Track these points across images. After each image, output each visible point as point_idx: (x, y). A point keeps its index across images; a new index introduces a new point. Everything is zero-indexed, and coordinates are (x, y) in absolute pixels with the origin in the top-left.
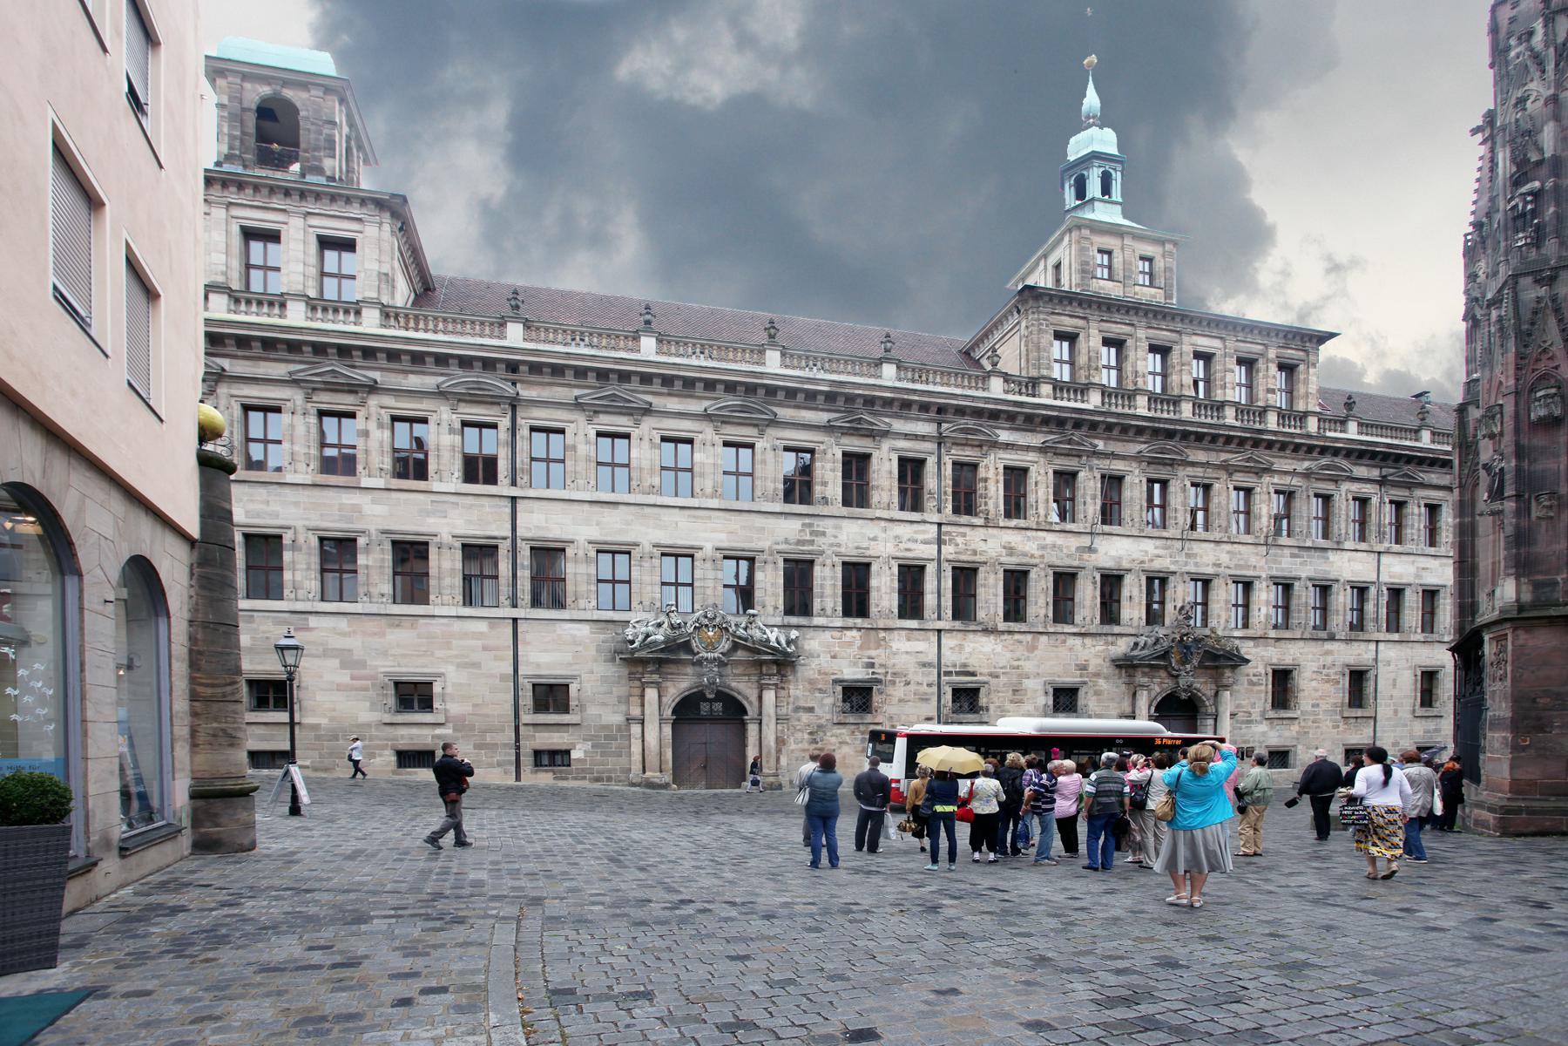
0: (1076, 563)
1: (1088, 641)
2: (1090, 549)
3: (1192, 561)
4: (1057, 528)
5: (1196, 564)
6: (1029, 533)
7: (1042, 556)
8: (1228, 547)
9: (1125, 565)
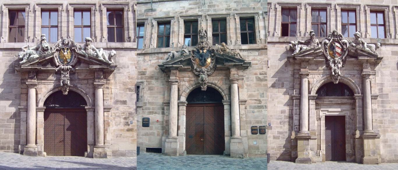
0: (144, 17)
1: (147, 58)
2: (152, 10)
3: (212, 9)
5: (215, 10)
9: (171, 15)
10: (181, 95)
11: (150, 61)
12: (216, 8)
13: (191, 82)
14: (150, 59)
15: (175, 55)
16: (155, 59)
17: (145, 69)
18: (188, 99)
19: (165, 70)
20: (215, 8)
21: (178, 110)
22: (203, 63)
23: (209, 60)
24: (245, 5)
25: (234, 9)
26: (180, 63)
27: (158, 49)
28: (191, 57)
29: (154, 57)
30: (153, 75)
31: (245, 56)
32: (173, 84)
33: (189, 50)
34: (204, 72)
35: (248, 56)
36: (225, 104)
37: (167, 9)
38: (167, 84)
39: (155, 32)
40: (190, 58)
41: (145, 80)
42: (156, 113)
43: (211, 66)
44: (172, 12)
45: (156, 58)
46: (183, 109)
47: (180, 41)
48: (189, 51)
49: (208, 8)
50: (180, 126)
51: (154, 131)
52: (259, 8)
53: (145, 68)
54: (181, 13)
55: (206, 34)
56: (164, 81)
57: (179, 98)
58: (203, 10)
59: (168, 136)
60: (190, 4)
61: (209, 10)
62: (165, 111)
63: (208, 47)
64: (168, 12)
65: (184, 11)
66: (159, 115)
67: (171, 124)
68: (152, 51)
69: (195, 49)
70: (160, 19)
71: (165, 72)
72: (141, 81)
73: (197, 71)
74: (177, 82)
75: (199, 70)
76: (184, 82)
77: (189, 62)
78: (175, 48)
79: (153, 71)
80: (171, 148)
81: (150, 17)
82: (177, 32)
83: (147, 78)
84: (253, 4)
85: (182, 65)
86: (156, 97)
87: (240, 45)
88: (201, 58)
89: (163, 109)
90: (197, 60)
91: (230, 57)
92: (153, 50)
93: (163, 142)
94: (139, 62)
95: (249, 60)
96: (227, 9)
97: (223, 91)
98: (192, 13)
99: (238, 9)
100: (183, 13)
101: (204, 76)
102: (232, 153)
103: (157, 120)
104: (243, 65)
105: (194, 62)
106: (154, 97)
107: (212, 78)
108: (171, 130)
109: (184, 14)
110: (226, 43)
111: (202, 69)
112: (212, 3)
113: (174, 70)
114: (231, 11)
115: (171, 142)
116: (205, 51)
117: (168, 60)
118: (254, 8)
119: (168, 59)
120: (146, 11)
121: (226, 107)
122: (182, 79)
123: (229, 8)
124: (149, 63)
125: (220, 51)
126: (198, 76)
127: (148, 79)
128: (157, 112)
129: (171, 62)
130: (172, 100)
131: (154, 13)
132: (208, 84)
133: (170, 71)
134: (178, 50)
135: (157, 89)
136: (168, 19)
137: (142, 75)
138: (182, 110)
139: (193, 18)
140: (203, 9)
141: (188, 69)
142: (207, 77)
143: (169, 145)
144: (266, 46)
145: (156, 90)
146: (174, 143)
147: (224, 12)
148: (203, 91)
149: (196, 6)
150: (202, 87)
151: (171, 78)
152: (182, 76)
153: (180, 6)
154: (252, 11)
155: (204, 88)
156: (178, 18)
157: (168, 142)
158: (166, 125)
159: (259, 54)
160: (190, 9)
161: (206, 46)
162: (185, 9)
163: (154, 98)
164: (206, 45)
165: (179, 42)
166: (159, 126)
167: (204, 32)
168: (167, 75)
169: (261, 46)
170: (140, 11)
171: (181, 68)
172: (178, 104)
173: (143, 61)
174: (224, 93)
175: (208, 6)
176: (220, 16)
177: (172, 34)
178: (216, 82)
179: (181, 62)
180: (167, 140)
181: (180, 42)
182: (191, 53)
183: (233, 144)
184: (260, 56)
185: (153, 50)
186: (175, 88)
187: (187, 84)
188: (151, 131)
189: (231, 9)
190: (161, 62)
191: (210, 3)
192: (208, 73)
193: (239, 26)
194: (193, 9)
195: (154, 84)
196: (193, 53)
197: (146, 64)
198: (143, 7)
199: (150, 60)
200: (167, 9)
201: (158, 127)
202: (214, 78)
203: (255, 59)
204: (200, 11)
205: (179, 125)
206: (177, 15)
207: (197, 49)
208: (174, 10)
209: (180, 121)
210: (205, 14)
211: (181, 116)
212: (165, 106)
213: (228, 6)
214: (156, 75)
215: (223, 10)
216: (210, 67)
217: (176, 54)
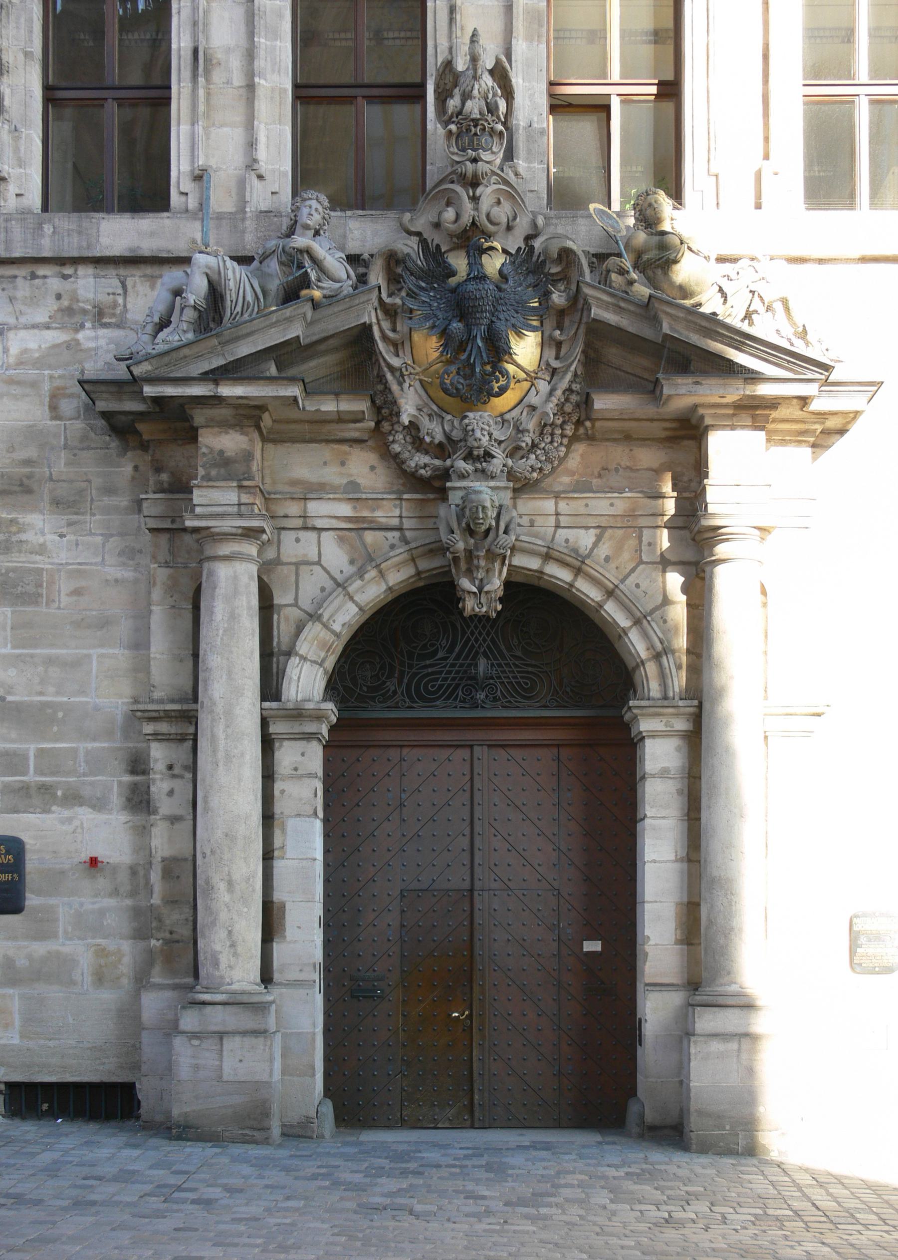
10: (289, 654)
13: (370, 537)
15: (230, 298)
16: (41, 317)
18: (339, 684)
19: (144, 425)
21: (268, 776)
22: (475, 367)
26: (273, 370)
27: (65, 222)
28: (370, 315)
29: (33, 301)
30: (28, 462)
32: (226, 549)
33: (354, 247)
34: (488, 456)
36: (654, 735)
38: (163, 555)
39: (28, 55)
40: (365, 330)
42: (73, 798)
43: (546, 397)
45: (52, 305)
46: (304, 764)
47: (262, 154)
48: (353, 259)
50: (283, 906)
51: (66, 950)
55: (502, 105)
56: (134, 519)
57: (270, 687)
59: (191, 988)
62: (160, 786)
63: (522, 226)
66: (102, 817)
67: (210, 887)
69: (409, 246)
71: (144, 446)
73: (418, 444)
74: (251, 534)
75: (439, 437)
76: (313, 535)
77: (358, 360)
79: (32, 434)
80: (220, 1078)
82: (236, 63)
85: (294, 391)
86: (76, 664)
88: (456, 326)
89: (138, 765)
90: (429, 347)
92: (14, 225)
93: (146, 1037)
97: (637, 622)
101: (488, 494)
102: (700, 1113)
103: (85, 856)
104: (816, 406)
105: (395, 362)
106: (50, 661)
107: (549, 505)
108: (214, 942)
111: (467, 432)
113: (225, 425)
115: (221, 1035)
116: (493, 264)
117: (170, 337)
119: (164, 324)
121: (660, 755)
122: (293, 509)
125: (622, 272)
126: (432, 487)
128: (86, 792)
129: (199, 357)
130: (216, 690)
132: (520, 561)
133: (191, 436)
134: (250, 243)
135: (77, 592)
138: (297, 775)
141: (341, 418)
142: (506, 497)
143: (208, 1058)
145: (65, 600)
146: (249, 1041)
148: (474, 617)
151: (198, 496)
152: (294, 483)
155: (482, 593)
157: (194, 1035)
158: (171, 901)
161: (502, 213)
163: (55, 672)
165: (251, 164)
166: (107, 906)
167: (487, 81)
168: (158, 470)
171: (293, 414)
172: (264, 723)
174: (645, 635)
177: (186, 85)
178: (585, 539)
179: (286, 355)
180: (189, 1020)
181: (264, 166)
182: (377, 277)
183: (716, 1046)
185: (16, 229)
186: (233, 586)
187: (336, 557)
188: (40, 949)
190: (100, 349)
192: (522, 466)
195: (42, 550)
196: (394, 279)
201: (102, 912)
202: (563, 506)
205: (278, 896)
207: (423, 242)
209: (278, 865)
211: (291, 823)
212: (157, 737)
214: (60, 465)
216: (533, 408)
217: (236, 277)
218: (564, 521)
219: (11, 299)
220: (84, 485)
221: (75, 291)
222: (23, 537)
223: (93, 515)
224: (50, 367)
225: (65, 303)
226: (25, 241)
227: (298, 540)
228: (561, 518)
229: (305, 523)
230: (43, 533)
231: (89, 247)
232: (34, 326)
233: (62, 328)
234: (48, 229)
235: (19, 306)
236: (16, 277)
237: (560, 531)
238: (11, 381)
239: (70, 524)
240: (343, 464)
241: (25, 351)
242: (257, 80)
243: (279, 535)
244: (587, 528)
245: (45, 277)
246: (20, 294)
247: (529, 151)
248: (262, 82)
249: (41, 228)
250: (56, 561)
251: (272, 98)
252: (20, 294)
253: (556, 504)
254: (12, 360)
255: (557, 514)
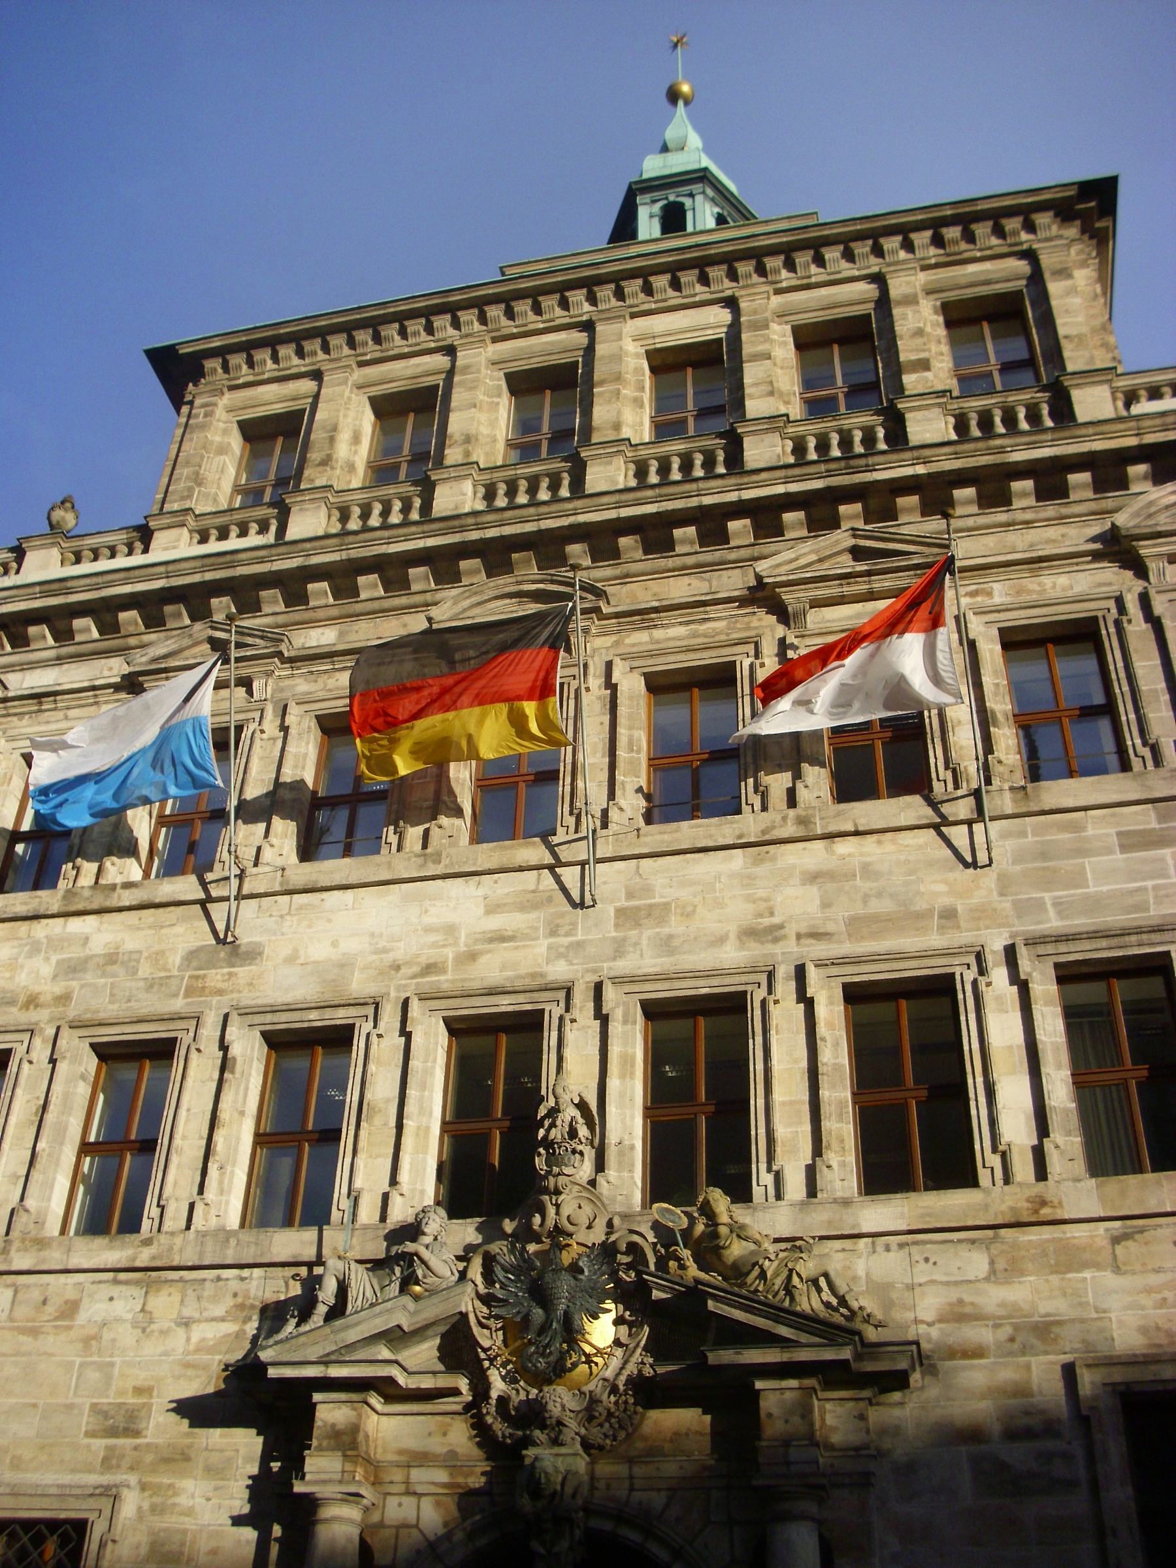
0: (178, 1004)
3: (646, 935)
4: (127, 898)
5: (667, 945)
6: (40, 930)
7: (64, 999)
8: (813, 855)
9: (359, 985)
11: (181, 1332)
12: (675, 926)
14: (187, 1312)
16: (219, 1311)
17: (139, 1391)
20: (666, 930)
23: (601, 1331)
24: (879, 895)
25: (803, 929)
27: (247, 1236)
29: (215, 1299)
31: (882, 1289)
35: (911, 1287)
37: (335, 944)
41: (133, 1479)
44: (366, 968)
45: (229, 1302)
49: (616, 926)
52: (983, 915)
53: (141, 1377)
54: (430, 968)
58: (579, 945)
60: (492, 909)
61: (624, 939)
64: (342, 966)
65: (450, 953)
68: (201, 1254)
70: (284, 1017)
72: (106, 1479)
78: (365, 1227)
81: (215, 1000)
83: (149, 1458)
84: (942, 888)
87: (846, 1203)
91: (751, 1303)
94: (107, 1336)
95: (916, 1321)
96: (750, 933)
98: (503, 968)
99: (830, 927)
100: (443, 971)
109: (449, 976)
110: (741, 1192)
112: (648, 890)
114: (777, 949)
118: (949, 915)
120: (191, 956)
123: (766, 921)
124: (178, 1341)
127: (153, 1469)
131: (243, 972)
132: (595, 1523)
136: (340, 1017)
137: (113, 1432)
139: (505, 1004)
140: (580, 937)
144: (1044, 1203)
147: (732, 955)
149: (533, 915)
150: (536, 1546)
153: (428, 920)
154: (936, 941)
156: (405, 1004)
159: (993, 1271)
160: (491, 940)
162: (456, 944)
164: (588, 1209)
169: (1009, 1202)
170: (157, 957)
173: (135, 1324)
175: (620, 912)
176: (704, 988)
184: (1007, 1282)
185: (209, 1242)
189: (781, 927)
191: (630, 895)
193: (836, 1054)
194: (511, 938)
197: (151, 1348)
198: (179, 929)
199: (186, 1323)
200: (335, 944)
203: (968, 1310)
204: (560, 956)
206: (399, 988)
208: (385, 951)
210: (594, 971)
213: (762, 906)
215: (722, 940)
218: (638, 1483)
219: (199, 1298)
220: (233, 1453)
221: (248, 1291)
222: (177, 1500)
223: (236, 1481)
224: (220, 1353)
225: (239, 1300)
226: (214, 1252)
227: (400, 1505)
228: (636, 1481)
229: (407, 1488)
230: (193, 1496)
231: (261, 1255)
232: (213, 1319)
233: (234, 1320)
234: (233, 1242)
235: (204, 1304)
236: (205, 1280)
237: (634, 1493)
238: (187, 1365)
239: (216, 1489)
240: (445, 1434)
241: (203, 1340)
242: (405, 1121)
243: (385, 1499)
244: (659, 1490)
245: (227, 1279)
246: (206, 1294)
247: (620, 1163)
248: (410, 1123)
249: (227, 1240)
250: (199, 1522)
251: (417, 1135)
252: (206, 1294)
253: (630, 1468)
254: (192, 1347)
255: (631, 1477)
